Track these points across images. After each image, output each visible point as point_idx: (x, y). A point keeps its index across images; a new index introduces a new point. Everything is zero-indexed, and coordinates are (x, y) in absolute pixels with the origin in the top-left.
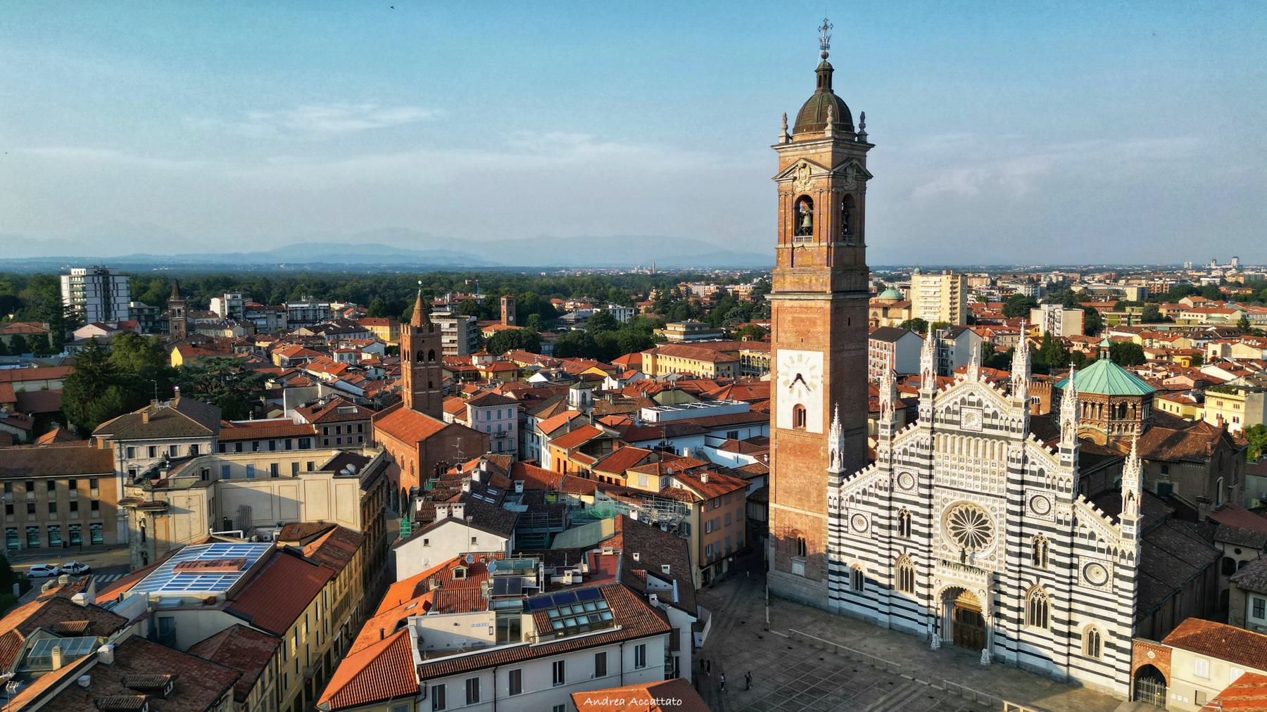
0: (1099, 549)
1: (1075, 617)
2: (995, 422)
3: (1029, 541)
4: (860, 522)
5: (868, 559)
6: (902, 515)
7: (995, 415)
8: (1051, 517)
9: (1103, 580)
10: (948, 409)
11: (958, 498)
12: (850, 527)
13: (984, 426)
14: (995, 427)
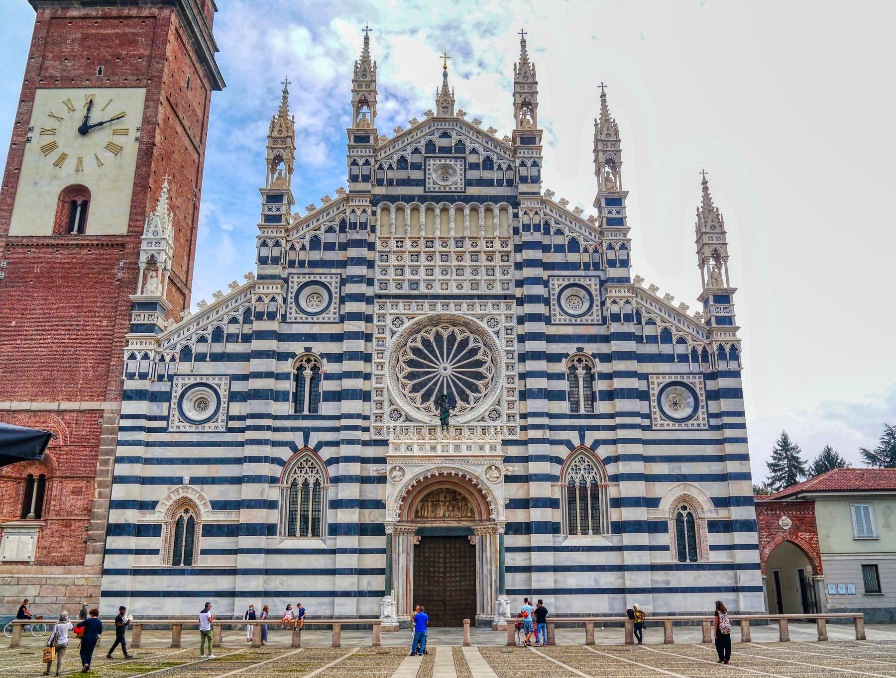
0: (679, 356)
1: (658, 489)
2: (487, 175)
3: (561, 367)
4: (201, 404)
5: (213, 481)
6: (301, 368)
7: (488, 164)
8: (595, 316)
9: (688, 411)
10: (402, 160)
11: (426, 311)
12: (175, 416)
13: (469, 183)
14: (489, 183)
